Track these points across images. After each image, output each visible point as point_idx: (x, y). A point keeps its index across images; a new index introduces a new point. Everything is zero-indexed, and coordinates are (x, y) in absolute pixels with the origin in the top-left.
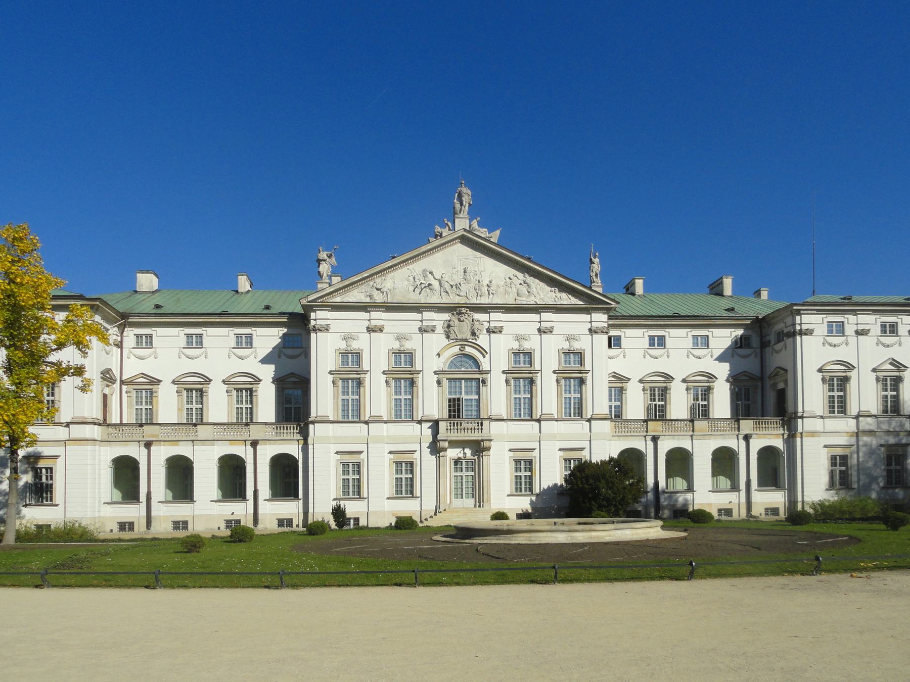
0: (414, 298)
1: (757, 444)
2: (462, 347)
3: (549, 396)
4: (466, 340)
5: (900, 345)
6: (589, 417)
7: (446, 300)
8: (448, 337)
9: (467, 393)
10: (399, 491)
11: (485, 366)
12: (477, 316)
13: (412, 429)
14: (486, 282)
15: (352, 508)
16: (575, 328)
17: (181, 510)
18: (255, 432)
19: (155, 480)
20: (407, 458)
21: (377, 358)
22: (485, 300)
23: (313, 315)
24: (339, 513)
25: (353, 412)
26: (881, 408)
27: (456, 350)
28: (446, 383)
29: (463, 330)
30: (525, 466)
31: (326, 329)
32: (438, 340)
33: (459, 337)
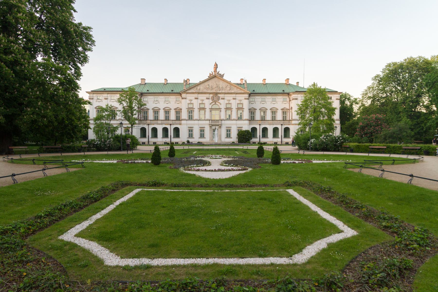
0: (205, 91)
1: (284, 127)
7: (212, 92)
10: (201, 136)
11: (221, 107)
12: (219, 95)
13: (204, 122)
14: (221, 87)
15: (191, 140)
17: (154, 140)
18: (170, 122)
19: (149, 133)
21: (196, 105)
22: (220, 92)
23: (183, 95)
24: (188, 142)
25: (190, 118)
30: (229, 131)
31: (186, 98)
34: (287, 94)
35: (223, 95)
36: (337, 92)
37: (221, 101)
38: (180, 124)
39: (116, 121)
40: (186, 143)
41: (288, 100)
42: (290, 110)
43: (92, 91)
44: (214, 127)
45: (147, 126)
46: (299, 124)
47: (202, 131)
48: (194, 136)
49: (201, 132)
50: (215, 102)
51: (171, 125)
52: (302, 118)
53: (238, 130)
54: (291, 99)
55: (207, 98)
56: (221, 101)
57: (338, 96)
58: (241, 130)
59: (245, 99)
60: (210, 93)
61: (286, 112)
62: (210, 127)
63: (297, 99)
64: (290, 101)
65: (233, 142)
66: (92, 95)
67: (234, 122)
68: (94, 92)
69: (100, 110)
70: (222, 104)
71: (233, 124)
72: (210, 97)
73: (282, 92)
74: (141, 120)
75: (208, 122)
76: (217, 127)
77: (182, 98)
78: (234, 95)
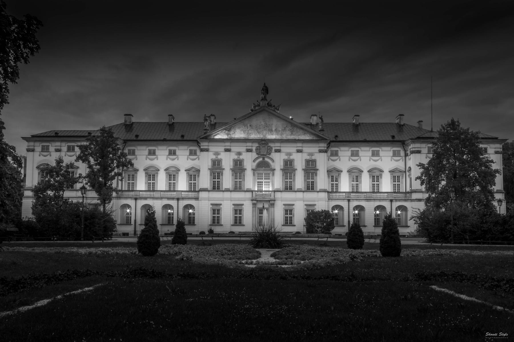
2: (264, 159)
3: (299, 182)
4: (265, 155)
5: (50, 156)
6: (318, 190)
8: (257, 154)
9: (265, 179)
12: (271, 145)
16: (312, 150)
20: (239, 208)
25: (216, 187)
26: (284, 187)
27: (261, 159)
28: (257, 175)
29: (264, 151)
30: (289, 211)
31: (207, 150)
32: (254, 155)
33: (262, 153)
34: (400, 143)
35: (278, 144)
36: (497, 138)
37: (274, 155)
38: (197, 199)
39: (75, 192)
40: (207, 233)
41: (402, 153)
42: (408, 174)
43: (33, 136)
44: (260, 206)
45: (134, 201)
46: (428, 200)
47: (238, 210)
48: (223, 221)
49: (236, 213)
50: (263, 156)
51: (178, 199)
52: (431, 188)
53: (308, 211)
54: (409, 152)
55: (248, 151)
56: (274, 155)
57: (499, 147)
58: (312, 211)
59: (321, 151)
60: (253, 141)
61: (398, 177)
62: (254, 204)
63: (419, 152)
64: (406, 155)
65: (298, 233)
66: (32, 144)
67: (300, 195)
68: (35, 138)
69: (46, 170)
70: (278, 161)
71: (296, 200)
72: (254, 149)
73: (391, 139)
74: (122, 191)
75: (249, 195)
76: (266, 206)
77: (202, 150)
78: (300, 145)
